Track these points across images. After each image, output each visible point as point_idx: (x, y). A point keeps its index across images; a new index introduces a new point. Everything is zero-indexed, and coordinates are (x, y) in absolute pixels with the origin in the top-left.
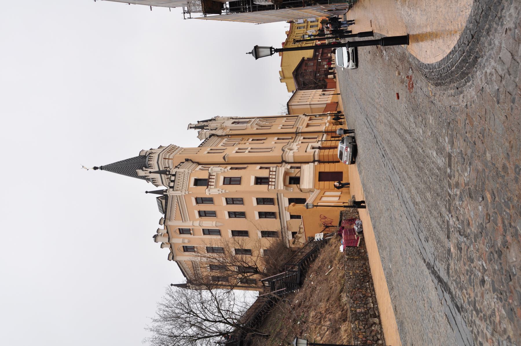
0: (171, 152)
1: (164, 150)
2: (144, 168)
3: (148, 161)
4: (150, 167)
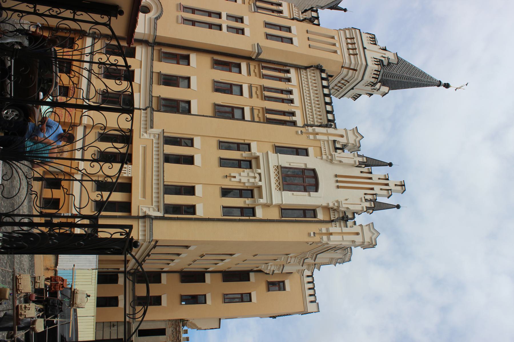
0: (343, 82)
1: (352, 89)
2: (385, 63)
3: (380, 72)
4: (378, 61)
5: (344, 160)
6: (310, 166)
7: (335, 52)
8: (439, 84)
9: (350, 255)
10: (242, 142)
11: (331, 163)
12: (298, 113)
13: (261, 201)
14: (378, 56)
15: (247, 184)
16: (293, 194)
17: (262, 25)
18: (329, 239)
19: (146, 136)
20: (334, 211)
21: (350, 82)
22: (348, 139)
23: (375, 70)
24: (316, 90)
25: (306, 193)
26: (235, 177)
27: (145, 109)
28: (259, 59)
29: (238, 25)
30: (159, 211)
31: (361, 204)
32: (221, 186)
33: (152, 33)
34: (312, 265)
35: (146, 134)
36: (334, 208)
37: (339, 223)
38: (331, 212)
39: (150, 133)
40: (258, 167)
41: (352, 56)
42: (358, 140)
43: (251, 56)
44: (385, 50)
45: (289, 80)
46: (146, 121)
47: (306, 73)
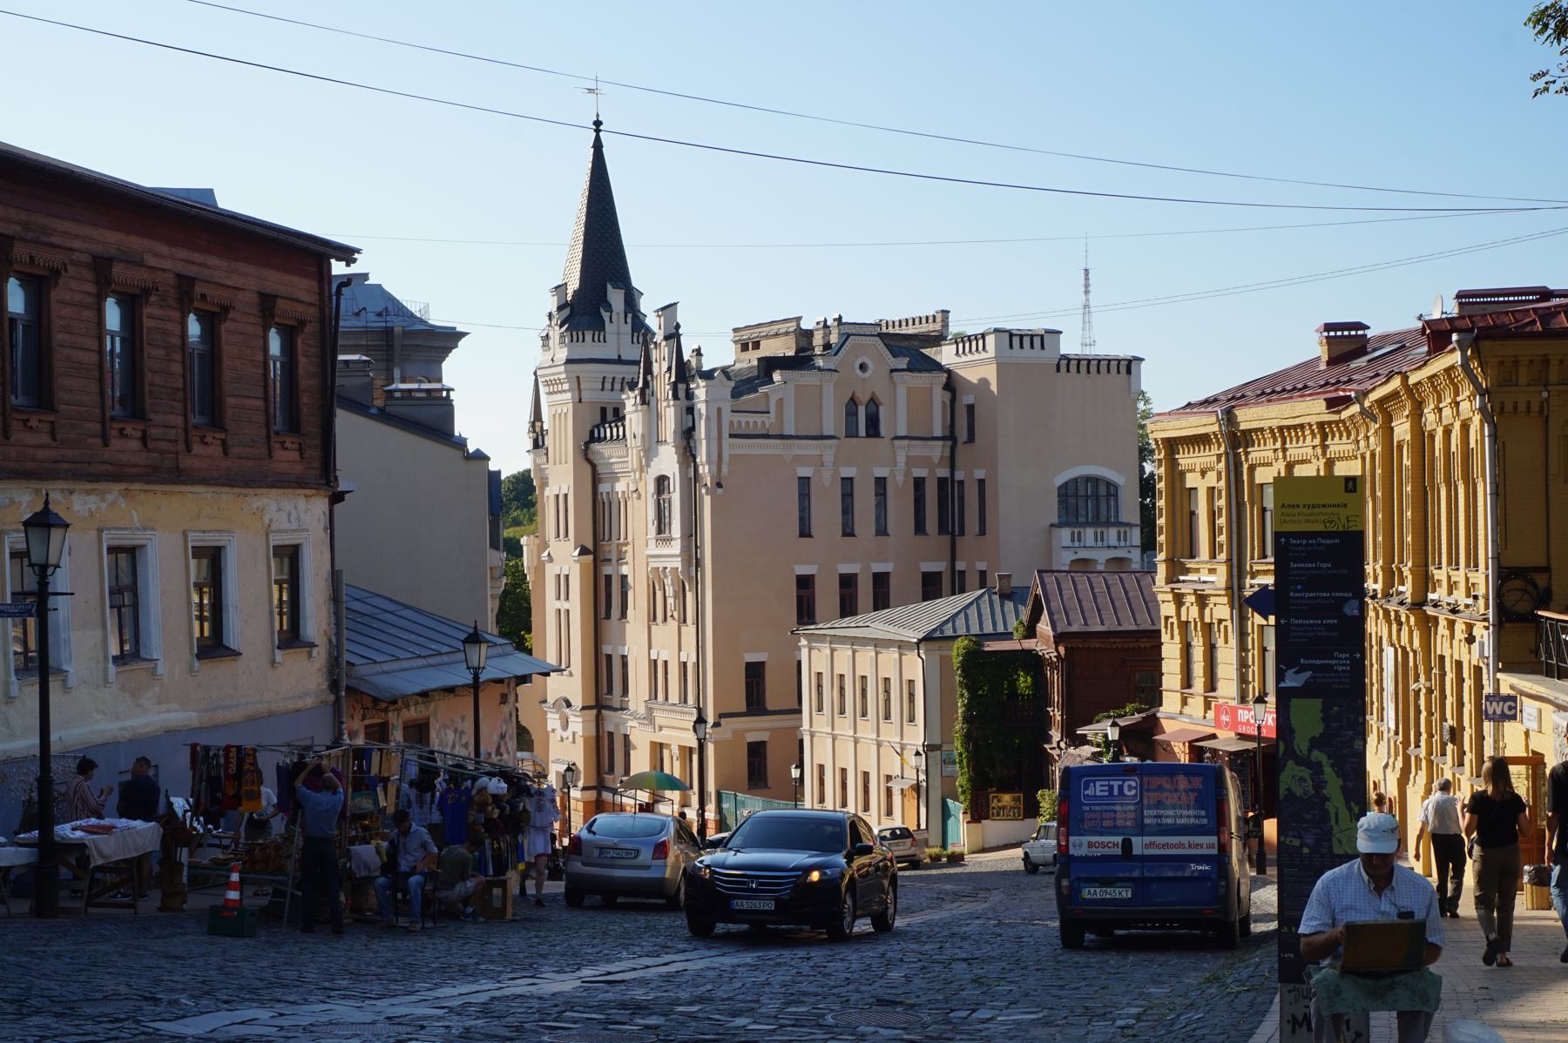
0: (608, 386)
2: (567, 312)
7: (566, 414)
8: (598, 146)
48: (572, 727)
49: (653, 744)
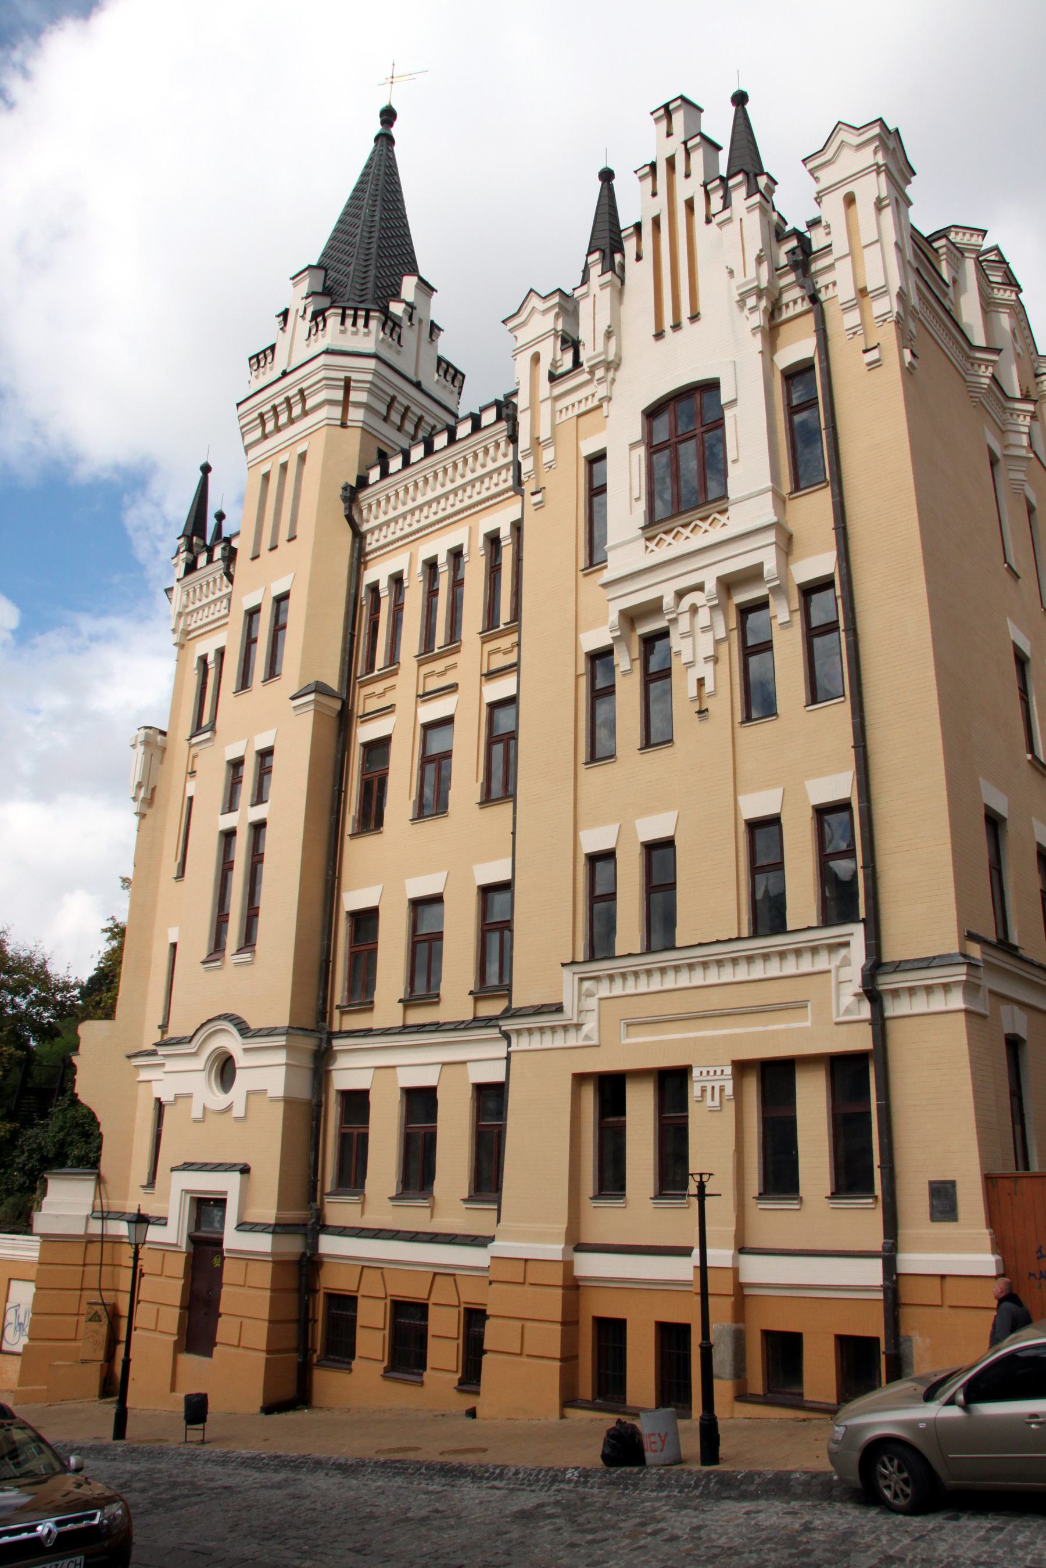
0: (396, 418)
1: (418, 385)
3: (344, 309)
4: (314, 323)
5: (604, 321)
6: (635, 429)
9: (957, 233)
10: (583, 682)
11: (619, 365)
12: (487, 524)
13: (770, 567)
14: (305, 325)
15: (721, 633)
16: (735, 461)
17: (246, 697)
18: (883, 291)
19: (591, 1025)
20: (780, 309)
21: (392, 392)
22: (540, 339)
23: (343, 323)
24: (416, 484)
25: (728, 414)
26: (701, 682)
27: (506, 1036)
28: (341, 688)
29: (249, 772)
30: (847, 944)
31: (741, 220)
32: (737, 725)
33: (281, 1040)
34: (1040, 385)
35: (582, 1025)
36: (765, 308)
37: (817, 276)
38: (785, 316)
39: (580, 1012)
40: (654, 608)
41: (308, 406)
42: (541, 305)
43: (334, 716)
44: (285, 314)
45: (397, 580)
46: (542, 1030)
47: (372, 531)
48: (243, 1082)
49: (580, 1079)
